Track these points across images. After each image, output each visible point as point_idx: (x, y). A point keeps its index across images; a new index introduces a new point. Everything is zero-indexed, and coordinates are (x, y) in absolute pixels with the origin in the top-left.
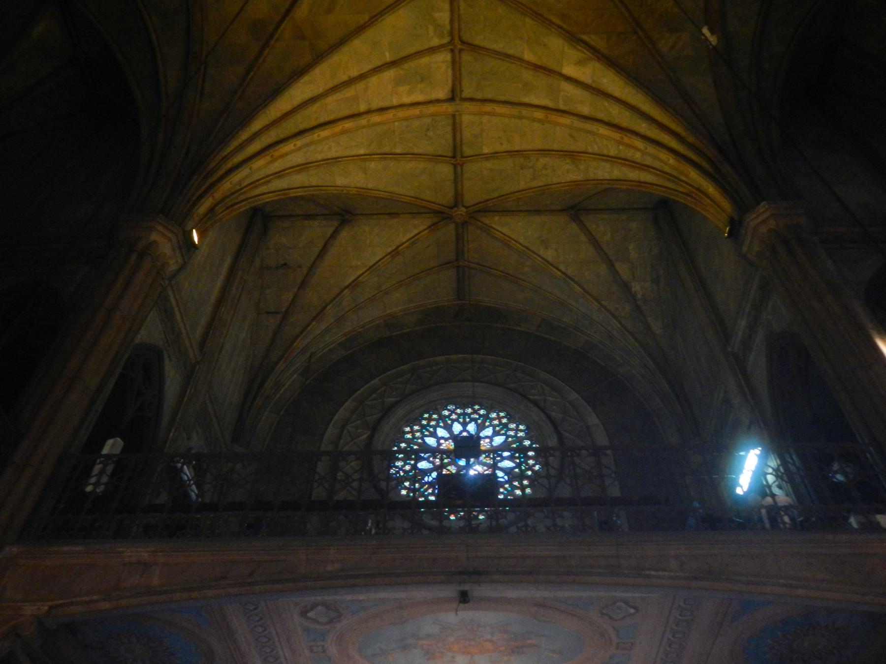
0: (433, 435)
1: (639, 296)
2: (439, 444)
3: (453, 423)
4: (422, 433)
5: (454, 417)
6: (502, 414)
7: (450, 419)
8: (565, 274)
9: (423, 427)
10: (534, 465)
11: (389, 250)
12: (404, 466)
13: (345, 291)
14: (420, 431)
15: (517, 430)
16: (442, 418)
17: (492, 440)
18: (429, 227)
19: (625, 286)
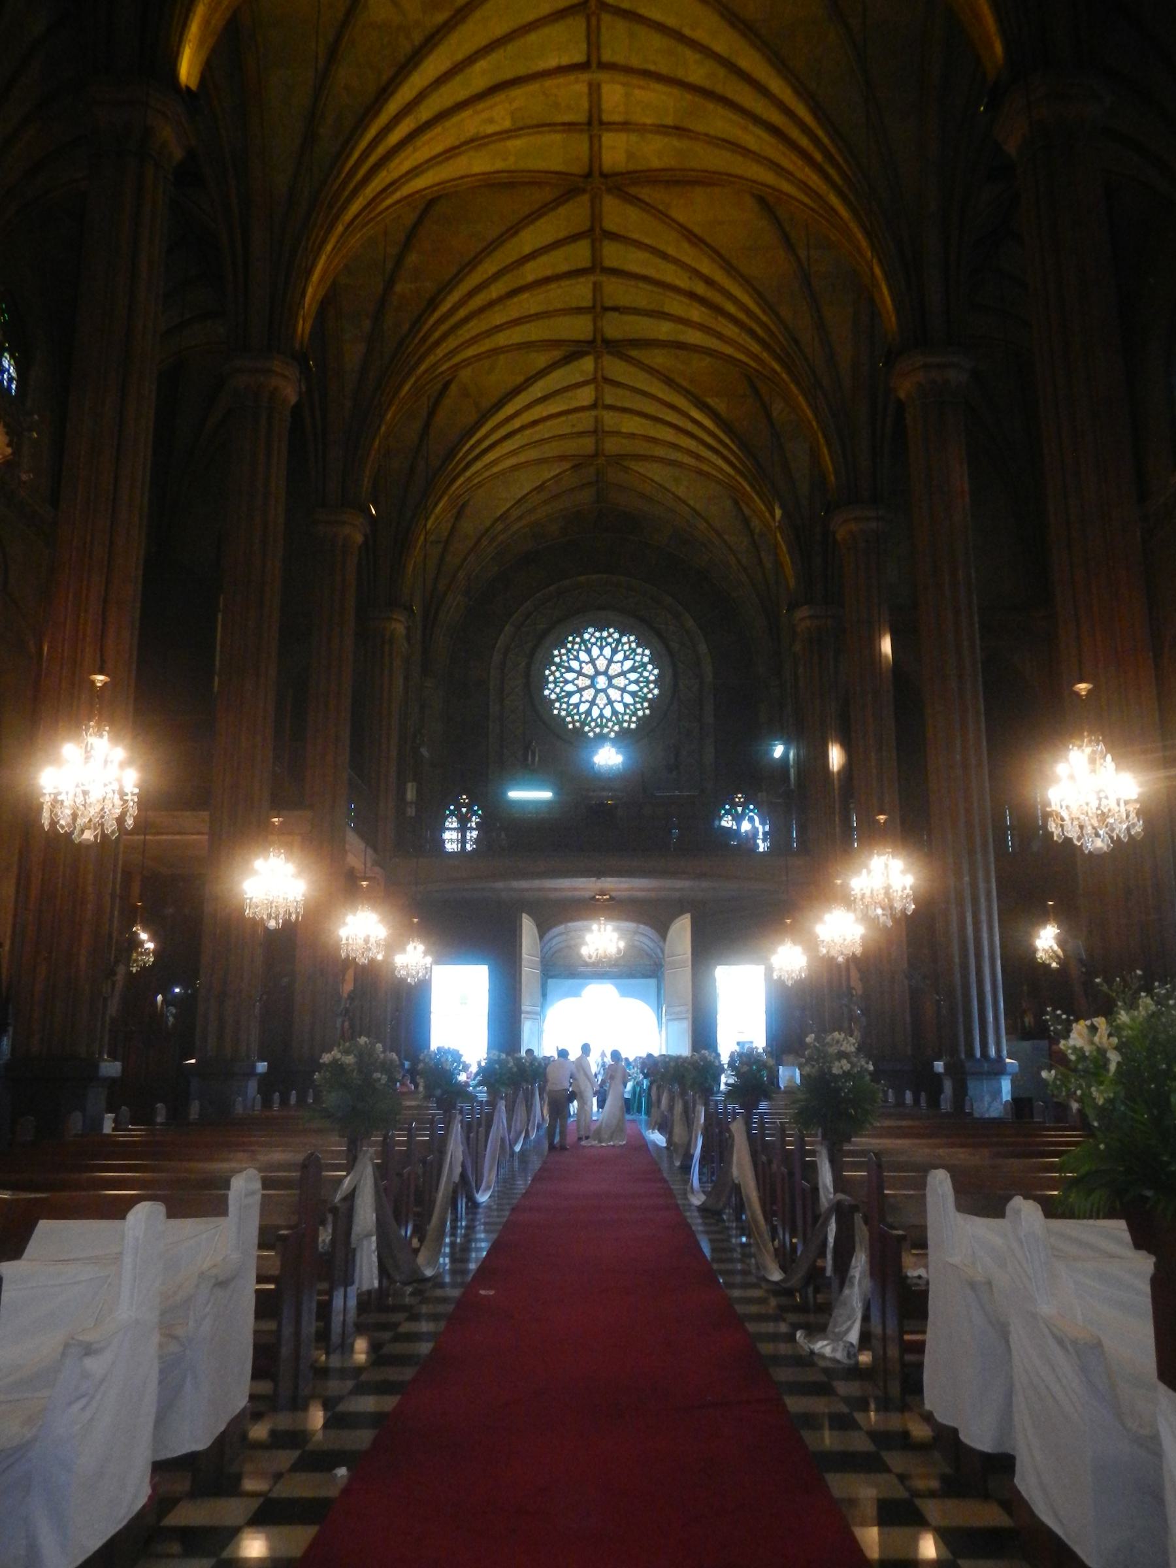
0: (577, 658)
1: (757, 531)
2: (581, 668)
4: (568, 657)
5: (593, 640)
6: (632, 638)
8: (694, 509)
9: (569, 651)
10: (653, 689)
12: (555, 688)
14: (566, 654)
15: (643, 655)
16: (583, 641)
17: (622, 665)
18: (573, 467)
19: (746, 521)
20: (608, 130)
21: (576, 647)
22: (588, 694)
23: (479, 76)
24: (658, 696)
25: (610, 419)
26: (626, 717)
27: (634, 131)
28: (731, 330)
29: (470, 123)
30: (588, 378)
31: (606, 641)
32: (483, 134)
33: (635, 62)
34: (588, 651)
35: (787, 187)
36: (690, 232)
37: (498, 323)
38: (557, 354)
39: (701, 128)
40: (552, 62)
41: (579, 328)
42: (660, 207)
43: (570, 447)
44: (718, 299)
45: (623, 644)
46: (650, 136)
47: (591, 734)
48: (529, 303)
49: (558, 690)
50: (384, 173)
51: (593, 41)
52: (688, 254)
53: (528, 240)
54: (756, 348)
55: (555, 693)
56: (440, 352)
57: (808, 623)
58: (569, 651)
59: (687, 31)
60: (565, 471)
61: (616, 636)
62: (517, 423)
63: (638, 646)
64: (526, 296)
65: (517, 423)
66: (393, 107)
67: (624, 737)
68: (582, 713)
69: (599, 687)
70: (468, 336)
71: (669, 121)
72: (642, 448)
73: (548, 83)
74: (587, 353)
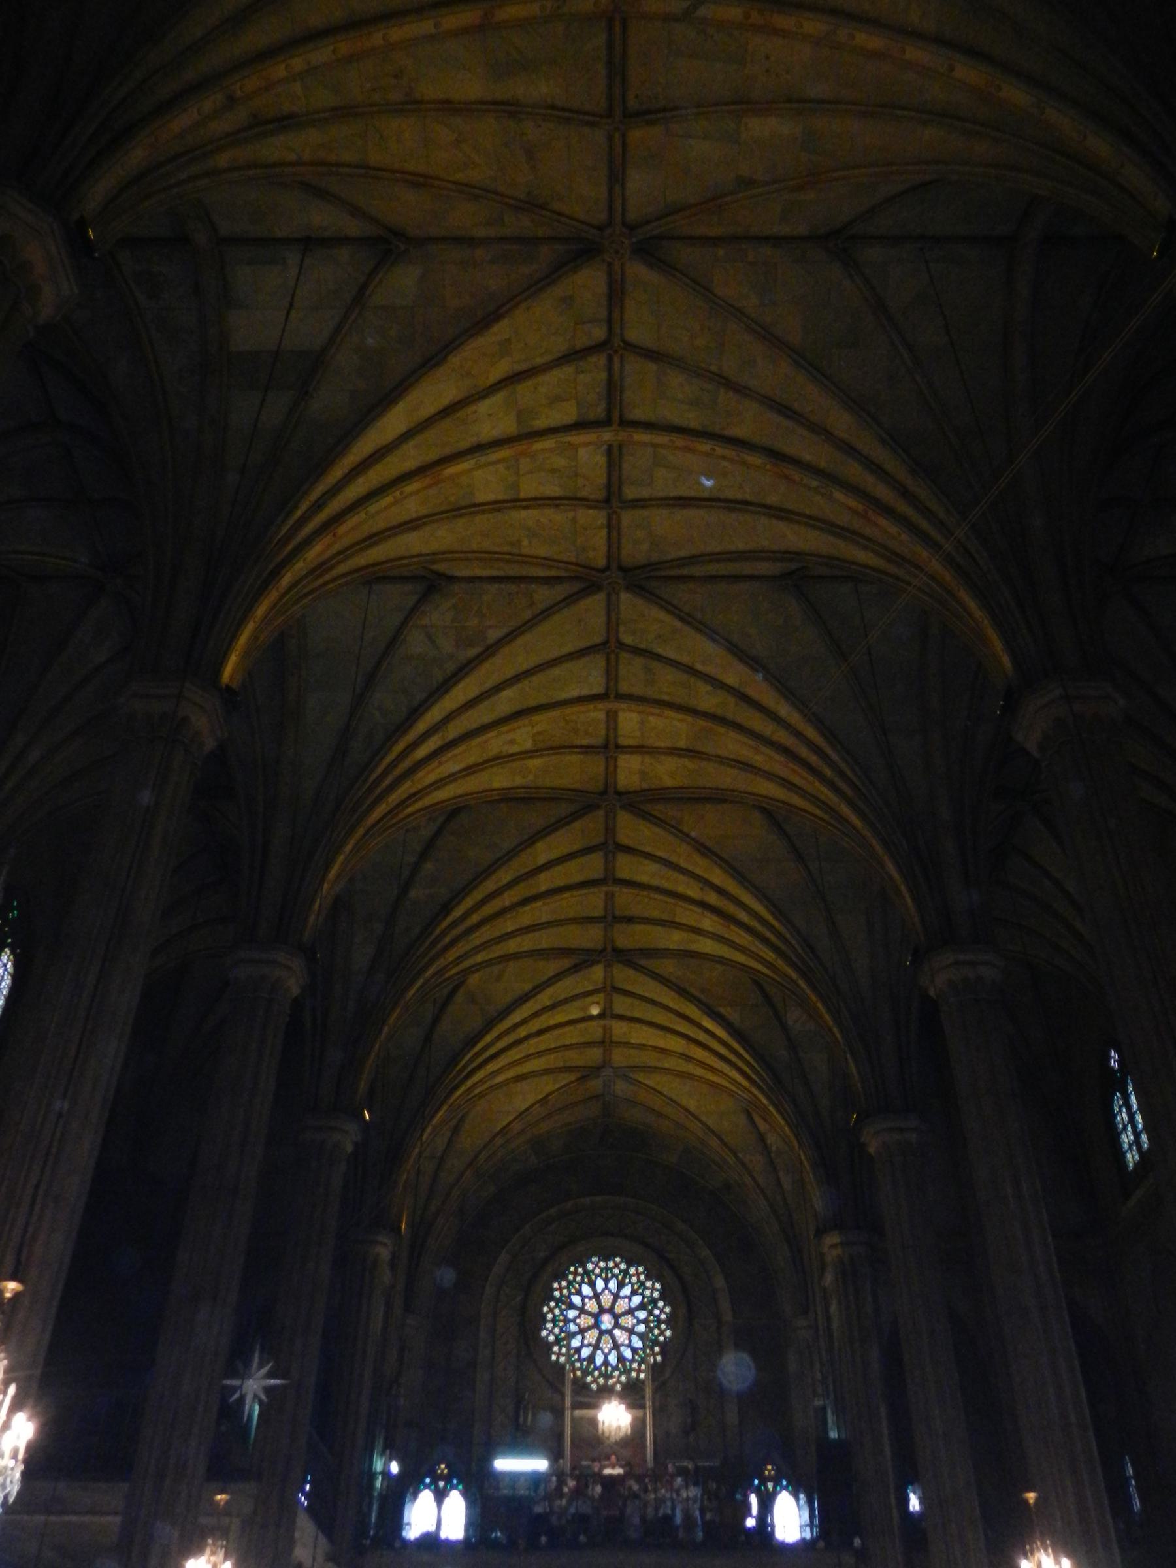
0: (579, 1292)
1: (774, 1148)
2: (584, 1304)
3: (596, 1278)
5: (597, 1271)
6: (641, 1269)
7: (594, 1274)
9: (570, 1283)
10: (665, 1330)
11: (540, 1097)
13: (496, 1139)
15: (653, 1289)
16: (587, 1273)
17: (630, 1300)
18: (578, 1079)
19: (762, 1138)
20: (622, 752)
21: (579, 1278)
22: (592, 1336)
23: (506, 702)
24: (671, 1339)
25: (619, 1029)
26: (635, 1365)
27: (648, 753)
28: (744, 938)
29: (495, 743)
30: (598, 987)
31: (611, 1272)
32: (504, 753)
33: (650, 693)
34: (592, 1285)
35: (796, 800)
36: (703, 845)
37: (509, 930)
38: (567, 963)
39: (709, 749)
40: (574, 693)
41: (590, 937)
42: (673, 823)
43: (576, 1058)
44: (731, 908)
45: (631, 1276)
46: (663, 757)
47: (594, 1386)
48: (541, 912)
49: (557, 1330)
50: (408, 784)
51: (611, 674)
52: (700, 865)
53: (543, 852)
54: (770, 955)
55: (554, 1334)
56: (452, 955)
57: (839, 1251)
58: (570, 1283)
59: (699, 667)
60: (572, 1082)
61: (623, 1266)
62: (522, 1032)
63: (648, 1278)
64: (539, 904)
65: (522, 1032)
66: (421, 726)
67: (632, 1394)
68: (584, 1360)
69: (603, 1327)
70: (478, 942)
71: (682, 744)
72: (650, 1059)
73: (568, 710)
74: (599, 962)
